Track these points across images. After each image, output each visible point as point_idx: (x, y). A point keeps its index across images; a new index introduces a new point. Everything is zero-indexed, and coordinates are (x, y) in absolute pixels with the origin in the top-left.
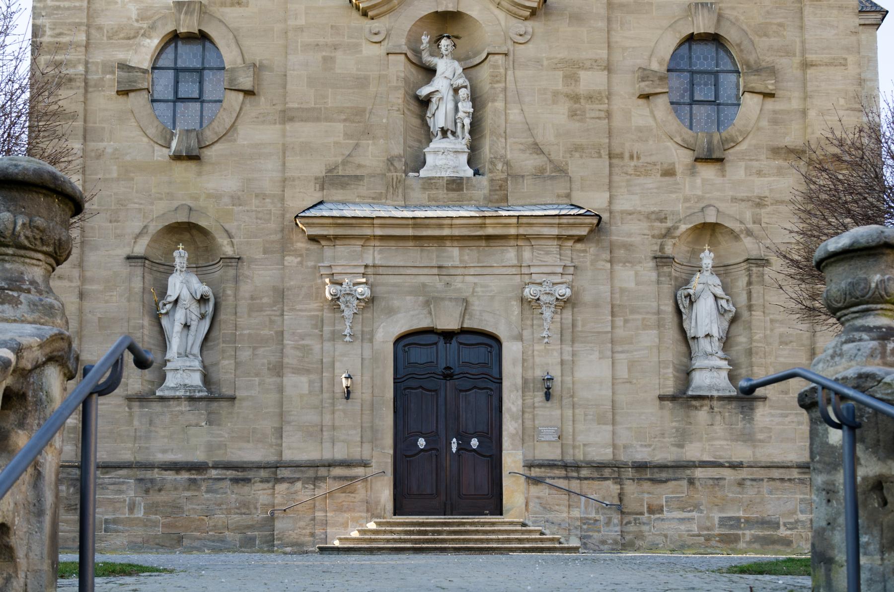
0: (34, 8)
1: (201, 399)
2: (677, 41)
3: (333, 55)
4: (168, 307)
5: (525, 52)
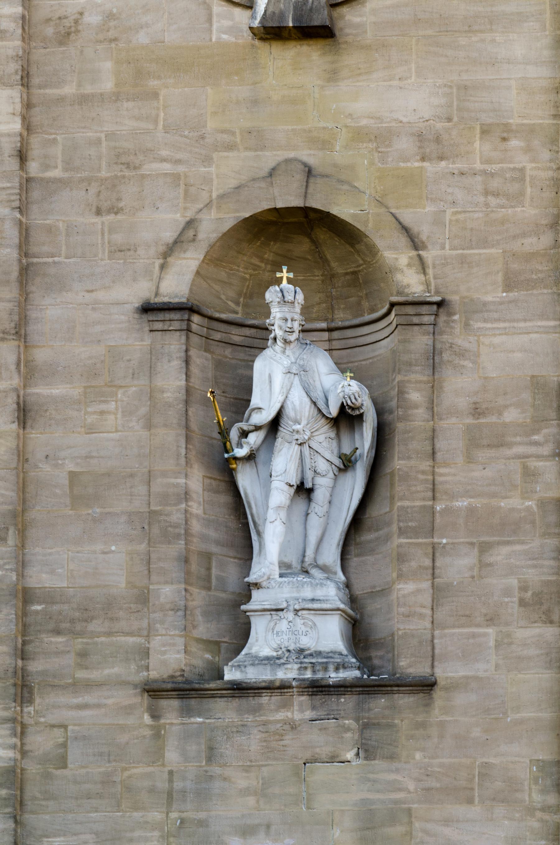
1: (342, 688)
4: (255, 439)
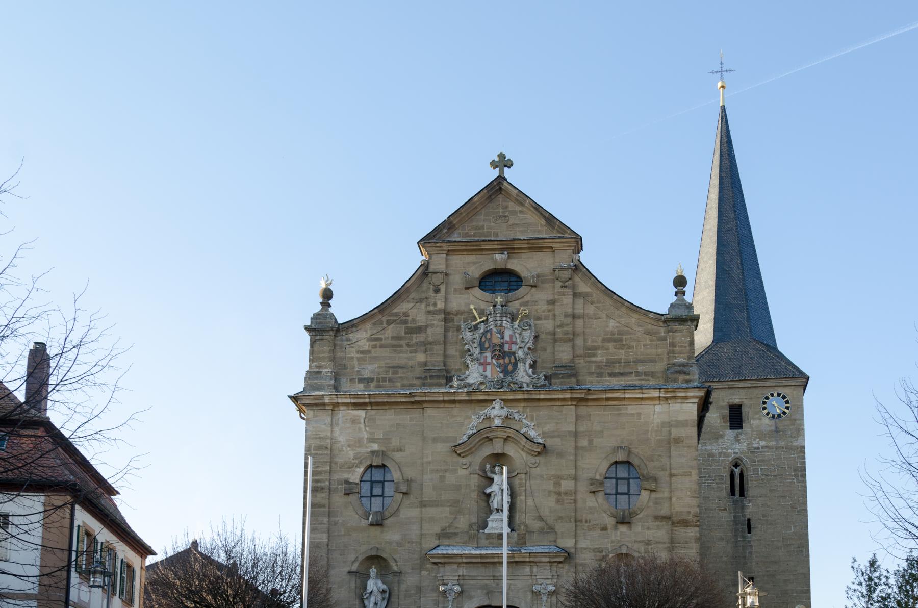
2: (608, 465)
5: (537, 471)
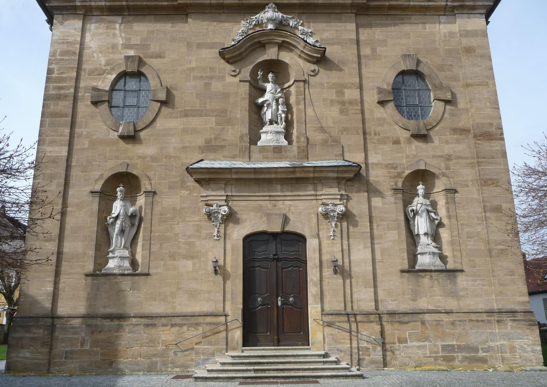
0: (49, 60)
1: (128, 275)
3: (210, 82)
